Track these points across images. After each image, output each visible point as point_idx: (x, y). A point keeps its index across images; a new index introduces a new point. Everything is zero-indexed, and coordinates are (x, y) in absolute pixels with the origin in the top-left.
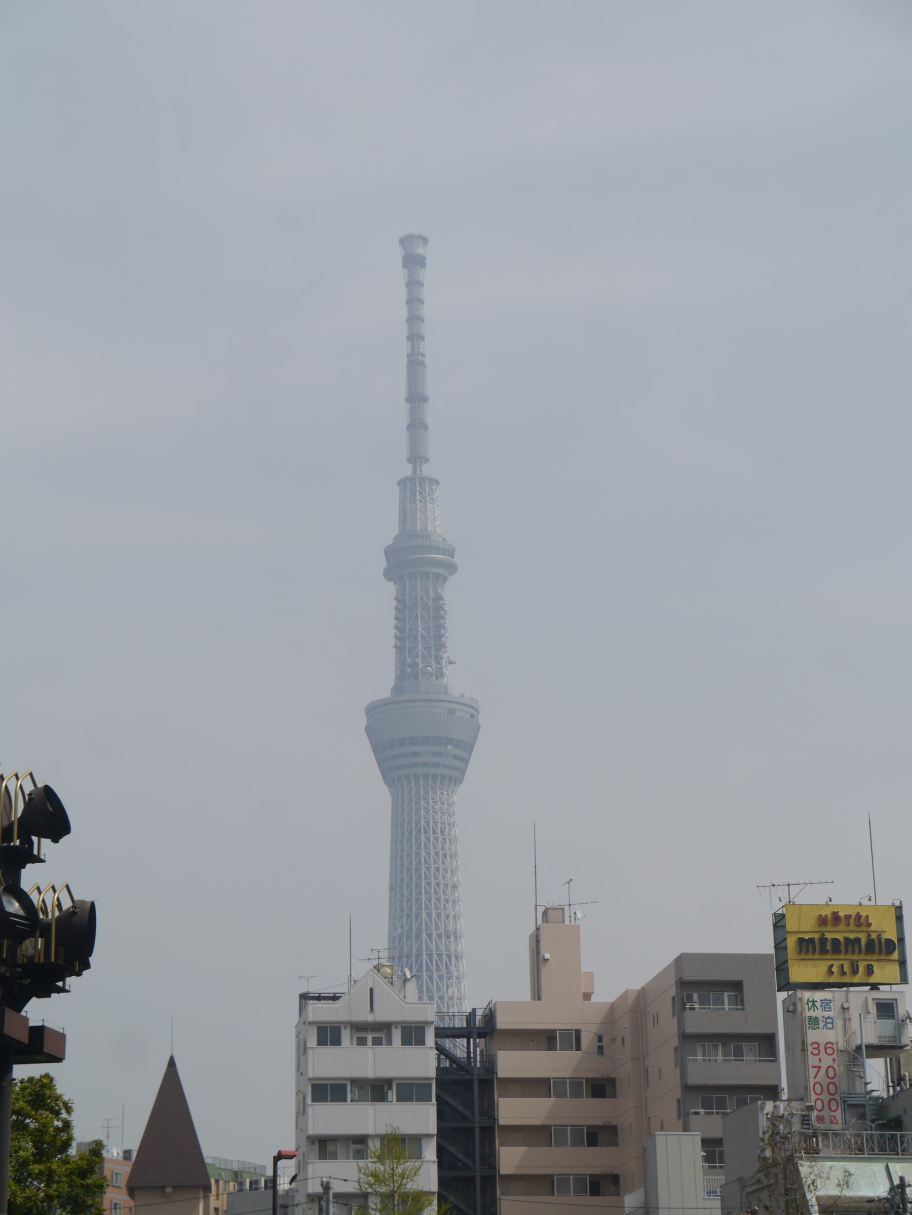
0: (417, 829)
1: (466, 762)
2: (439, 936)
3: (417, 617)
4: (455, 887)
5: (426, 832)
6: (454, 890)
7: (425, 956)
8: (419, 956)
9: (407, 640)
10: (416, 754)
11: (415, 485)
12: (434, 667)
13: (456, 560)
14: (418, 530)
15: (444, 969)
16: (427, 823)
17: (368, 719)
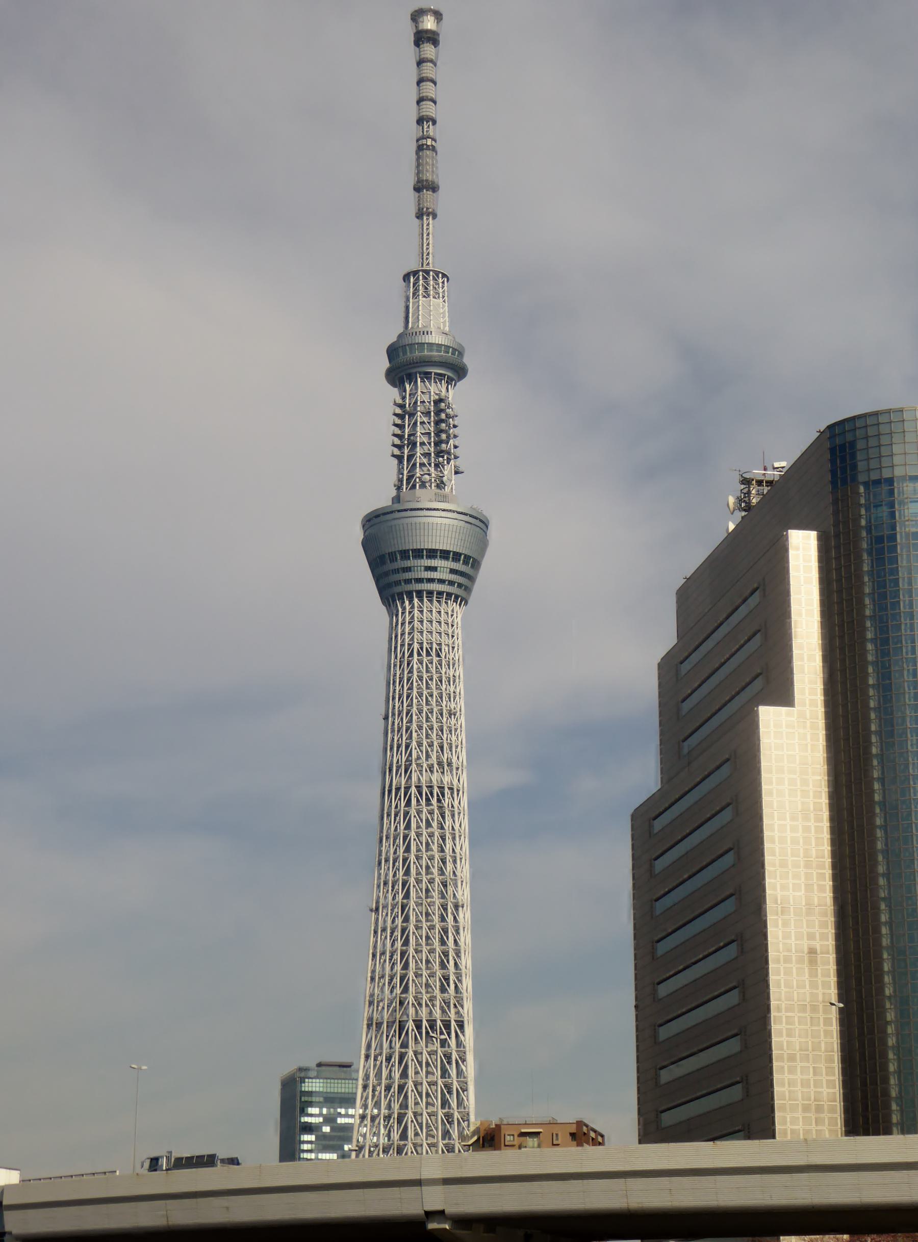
0: (410, 651)
1: (471, 578)
2: (431, 767)
3: (415, 423)
4: (451, 714)
5: (419, 654)
6: (450, 717)
7: (413, 790)
8: (407, 789)
9: (406, 447)
10: (408, 569)
11: (418, 279)
12: (433, 475)
13: (467, 360)
14: (420, 326)
15: (434, 801)
16: (421, 644)
17: (364, 533)
